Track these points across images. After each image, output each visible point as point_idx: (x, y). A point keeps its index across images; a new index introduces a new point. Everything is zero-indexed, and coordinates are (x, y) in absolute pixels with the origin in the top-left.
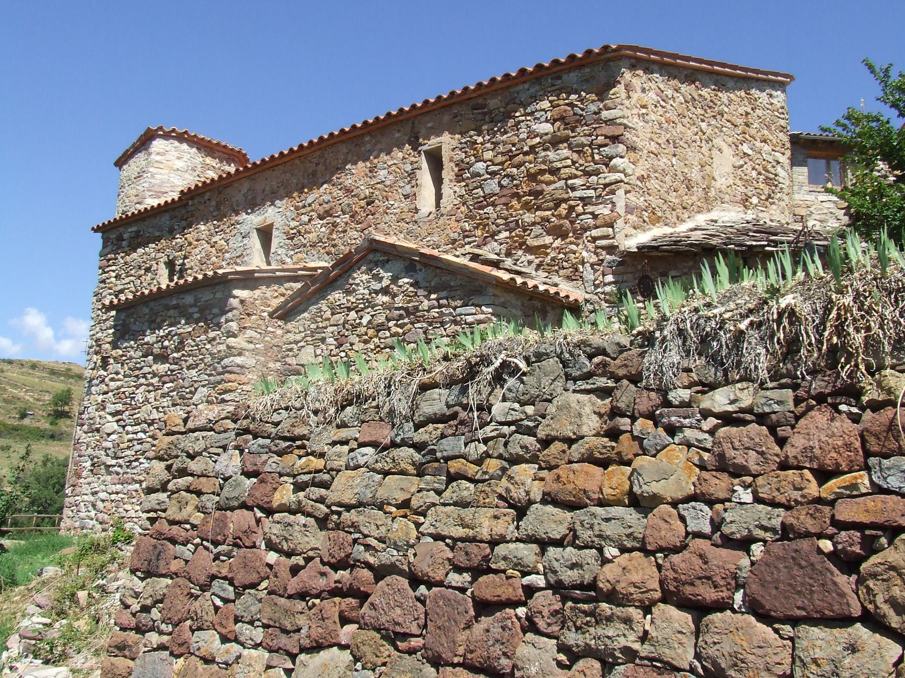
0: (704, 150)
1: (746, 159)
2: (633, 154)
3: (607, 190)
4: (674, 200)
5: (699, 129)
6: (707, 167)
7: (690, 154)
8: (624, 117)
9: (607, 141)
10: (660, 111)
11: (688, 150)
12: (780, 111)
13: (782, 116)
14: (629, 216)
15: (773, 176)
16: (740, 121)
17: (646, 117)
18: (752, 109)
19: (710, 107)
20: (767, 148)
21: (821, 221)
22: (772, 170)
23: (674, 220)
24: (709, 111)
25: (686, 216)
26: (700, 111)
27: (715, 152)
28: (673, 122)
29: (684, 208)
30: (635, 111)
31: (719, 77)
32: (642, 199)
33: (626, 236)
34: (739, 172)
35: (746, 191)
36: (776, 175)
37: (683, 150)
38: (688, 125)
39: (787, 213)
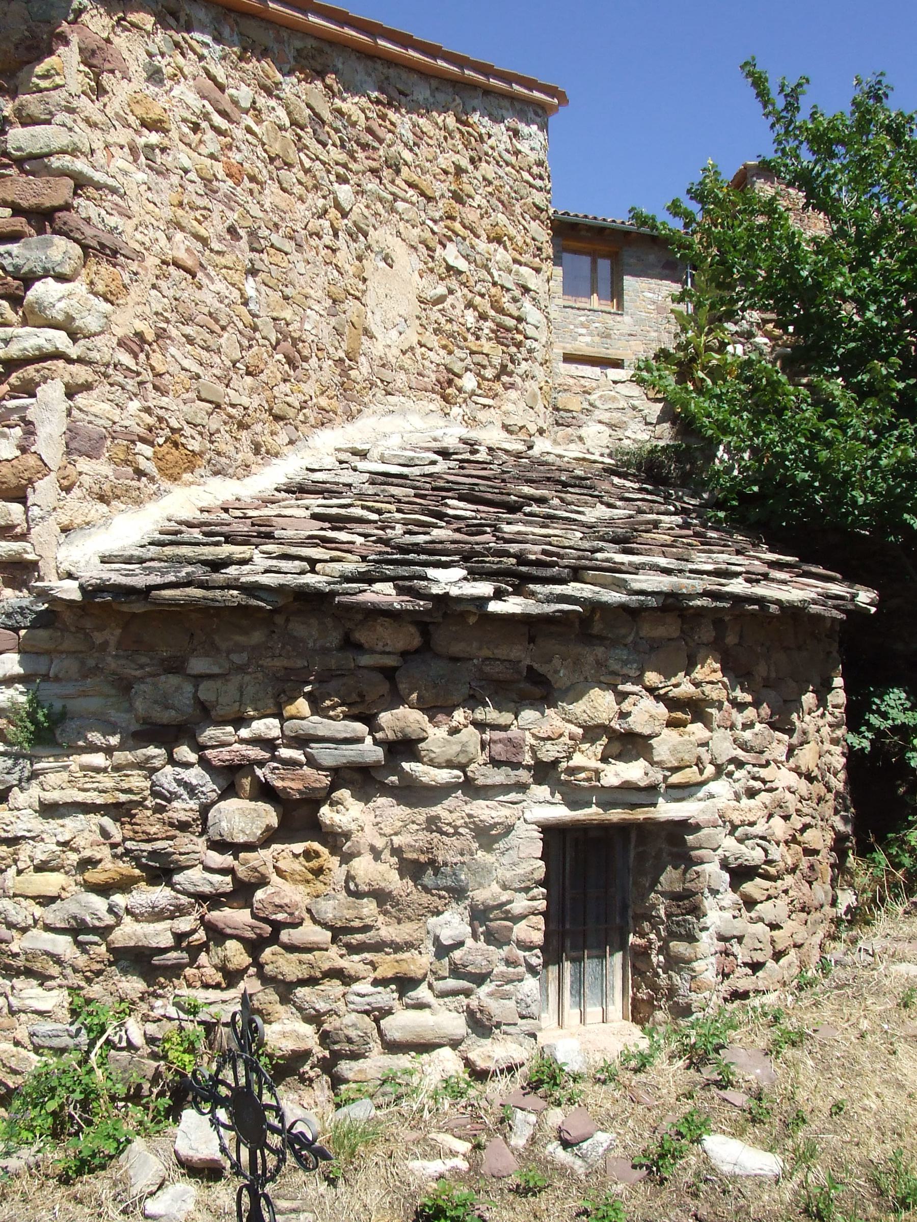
0: (344, 257)
1: (454, 283)
2: (105, 269)
3: (13, 379)
4: (245, 401)
5: (330, 202)
6: (351, 304)
7: (301, 267)
8: (74, 151)
9: (20, 224)
10: (212, 142)
11: (295, 256)
12: (535, 170)
13: (538, 183)
14: (83, 464)
15: (511, 323)
16: (439, 188)
17: (159, 157)
18: (472, 161)
19: (365, 147)
20: (502, 255)
21: (612, 426)
22: (512, 308)
23: (246, 454)
24: (360, 155)
25: (283, 438)
26: (337, 154)
27: (373, 263)
28: (253, 179)
29: (278, 418)
30: (122, 136)
31: (392, 72)
32: (134, 406)
33: (65, 530)
34: (434, 314)
35: (448, 360)
36: (520, 319)
37: (278, 258)
38: (298, 190)
39: (539, 407)
